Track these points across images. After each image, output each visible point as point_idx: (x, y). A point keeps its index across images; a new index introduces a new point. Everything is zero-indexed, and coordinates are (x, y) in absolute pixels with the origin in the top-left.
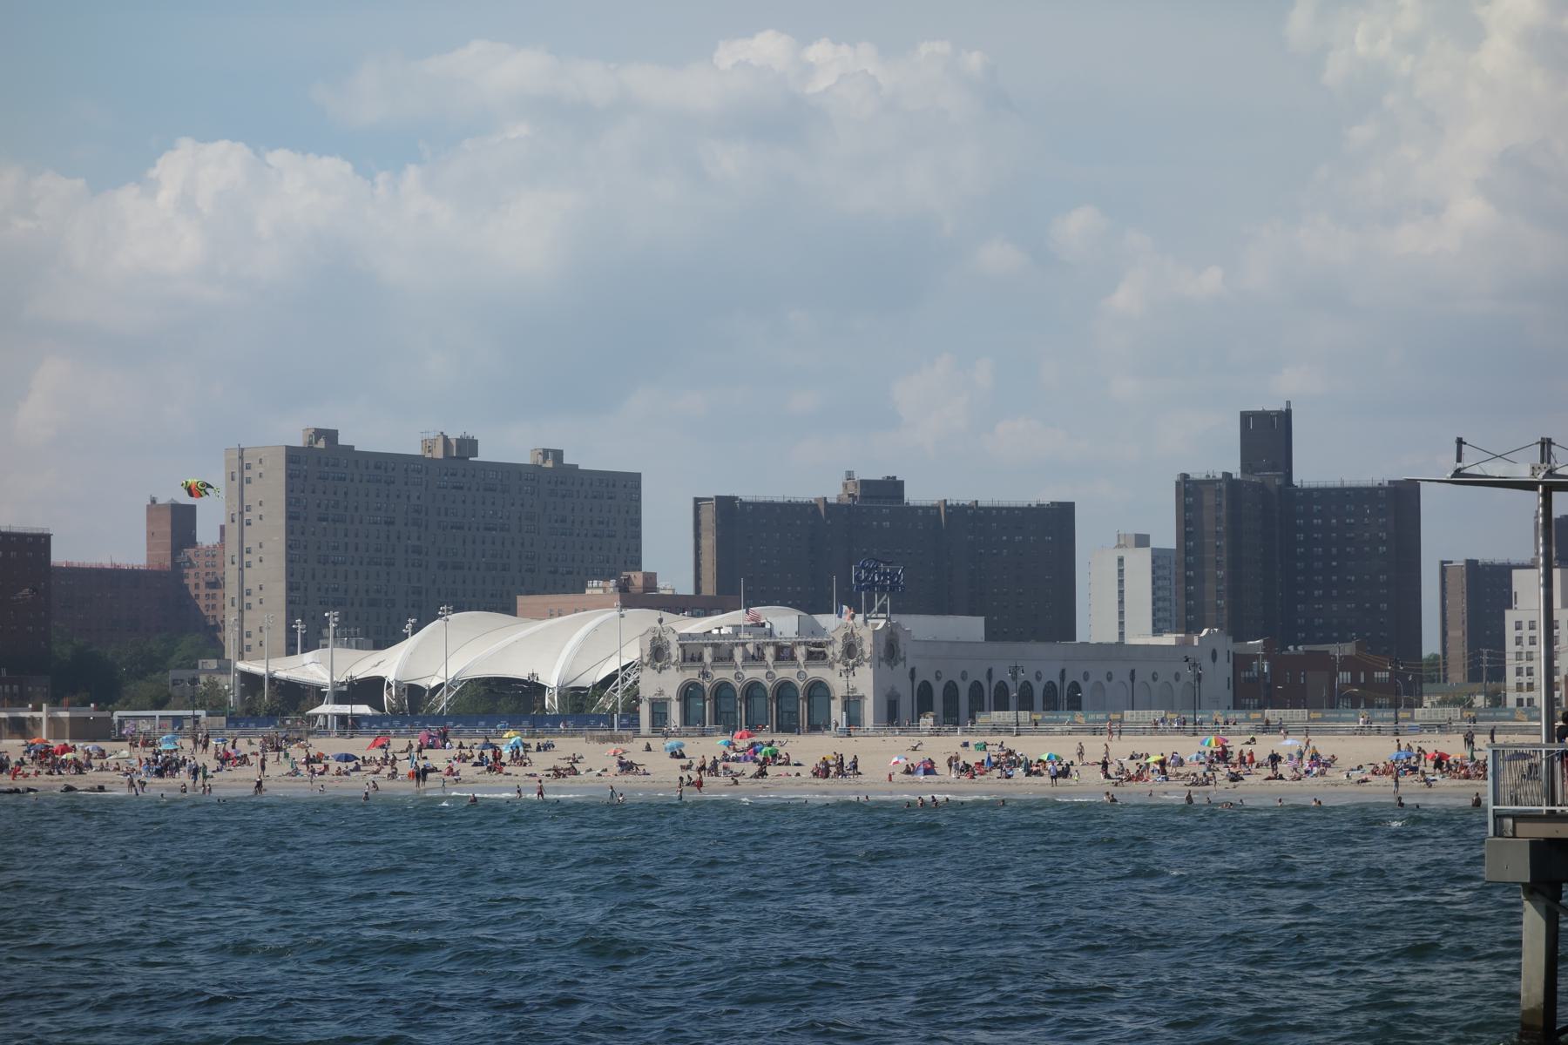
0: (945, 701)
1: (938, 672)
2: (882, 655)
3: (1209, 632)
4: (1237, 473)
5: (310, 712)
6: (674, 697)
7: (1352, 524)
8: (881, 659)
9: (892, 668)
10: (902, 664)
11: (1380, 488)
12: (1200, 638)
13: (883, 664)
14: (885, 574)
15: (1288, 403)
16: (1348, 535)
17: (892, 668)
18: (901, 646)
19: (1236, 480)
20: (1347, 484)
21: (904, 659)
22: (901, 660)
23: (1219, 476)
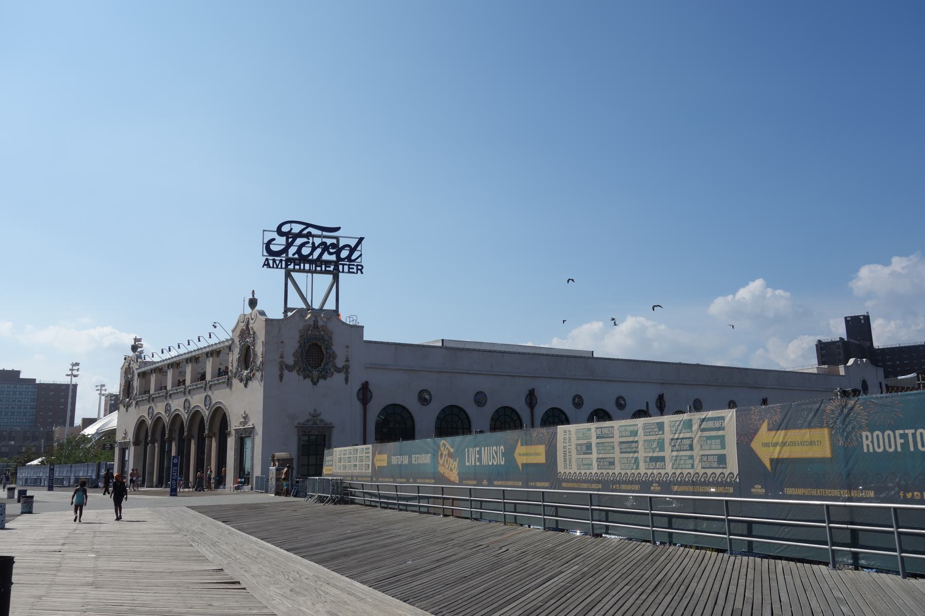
0: (70, 419)
1: (422, 392)
2: (290, 361)
3: (855, 362)
4: (845, 337)
5: (28, 464)
6: (132, 441)
7: (907, 363)
8: (283, 367)
9: (315, 383)
10: (339, 378)
11: (920, 346)
12: (847, 368)
13: (292, 377)
14: (325, 248)
15: (867, 312)
16: (906, 368)
17: (315, 383)
18: (338, 348)
19: (846, 341)
20: (902, 345)
21: (346, 369)
22: (339, 370)
23: (838, 339)
